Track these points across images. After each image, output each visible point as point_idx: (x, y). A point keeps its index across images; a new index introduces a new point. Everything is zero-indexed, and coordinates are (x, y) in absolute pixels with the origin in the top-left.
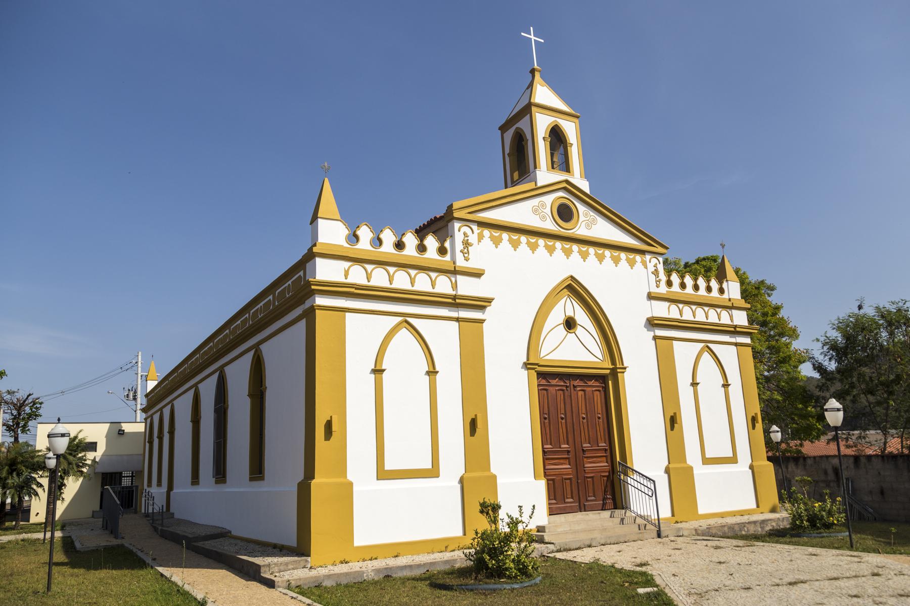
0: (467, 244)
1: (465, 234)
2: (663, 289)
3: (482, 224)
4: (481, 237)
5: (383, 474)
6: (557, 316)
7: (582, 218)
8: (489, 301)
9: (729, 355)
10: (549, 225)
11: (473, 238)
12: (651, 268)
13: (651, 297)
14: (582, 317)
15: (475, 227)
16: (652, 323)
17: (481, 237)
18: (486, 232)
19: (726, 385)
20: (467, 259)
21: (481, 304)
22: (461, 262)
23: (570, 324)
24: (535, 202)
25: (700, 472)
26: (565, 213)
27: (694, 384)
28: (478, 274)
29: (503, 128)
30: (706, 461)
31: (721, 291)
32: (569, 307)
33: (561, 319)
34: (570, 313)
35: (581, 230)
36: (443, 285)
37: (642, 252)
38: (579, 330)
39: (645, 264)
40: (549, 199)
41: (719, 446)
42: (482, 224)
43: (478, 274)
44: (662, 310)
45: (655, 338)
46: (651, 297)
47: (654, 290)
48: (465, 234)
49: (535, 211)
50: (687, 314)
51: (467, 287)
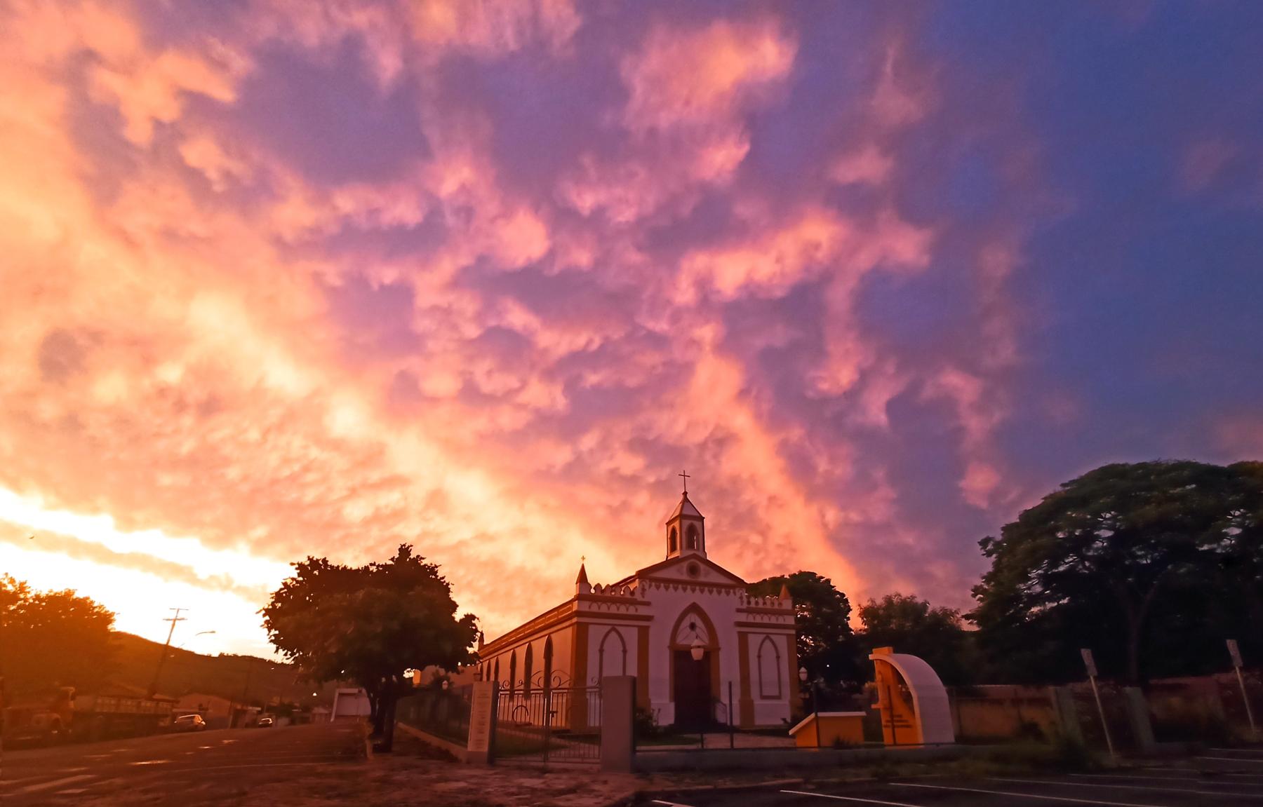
2: (745, 606)
3: (652, 580)
4: (650, 586)
6: (686, 622)
9: (782, 642)
10: (685, 577)
11: (647, 587)
12: (738, 595)
13: (739, 610)
14: (699, 623)
16: (739, 624)
17: (650, 586)
18: (653, 584)
19: (778, 657)
20: (643, 597)
21: (649, 618)
23: (693, 626)
25: (758, 702)
26: (693, 570)
27: (759, 657)
28: (648, 604)
29: (668, 524)
30: (763, 697)
31: (780, 604)
32: (693, 618)
33: (688, 624)
34: (693, 621)
35: (702, 579)
36: (632, 611)
37: (733, 587)
38: (698, 630)
39: (735, 593)
40: (685, 565)
41: (771, 690)
42: (652, 580)
43: (648, 604)
44: (743, 618)
45: (739, 632)
46: (739, 610)
47: (740, 607)
50: (758, 619)
51: (643, 611)
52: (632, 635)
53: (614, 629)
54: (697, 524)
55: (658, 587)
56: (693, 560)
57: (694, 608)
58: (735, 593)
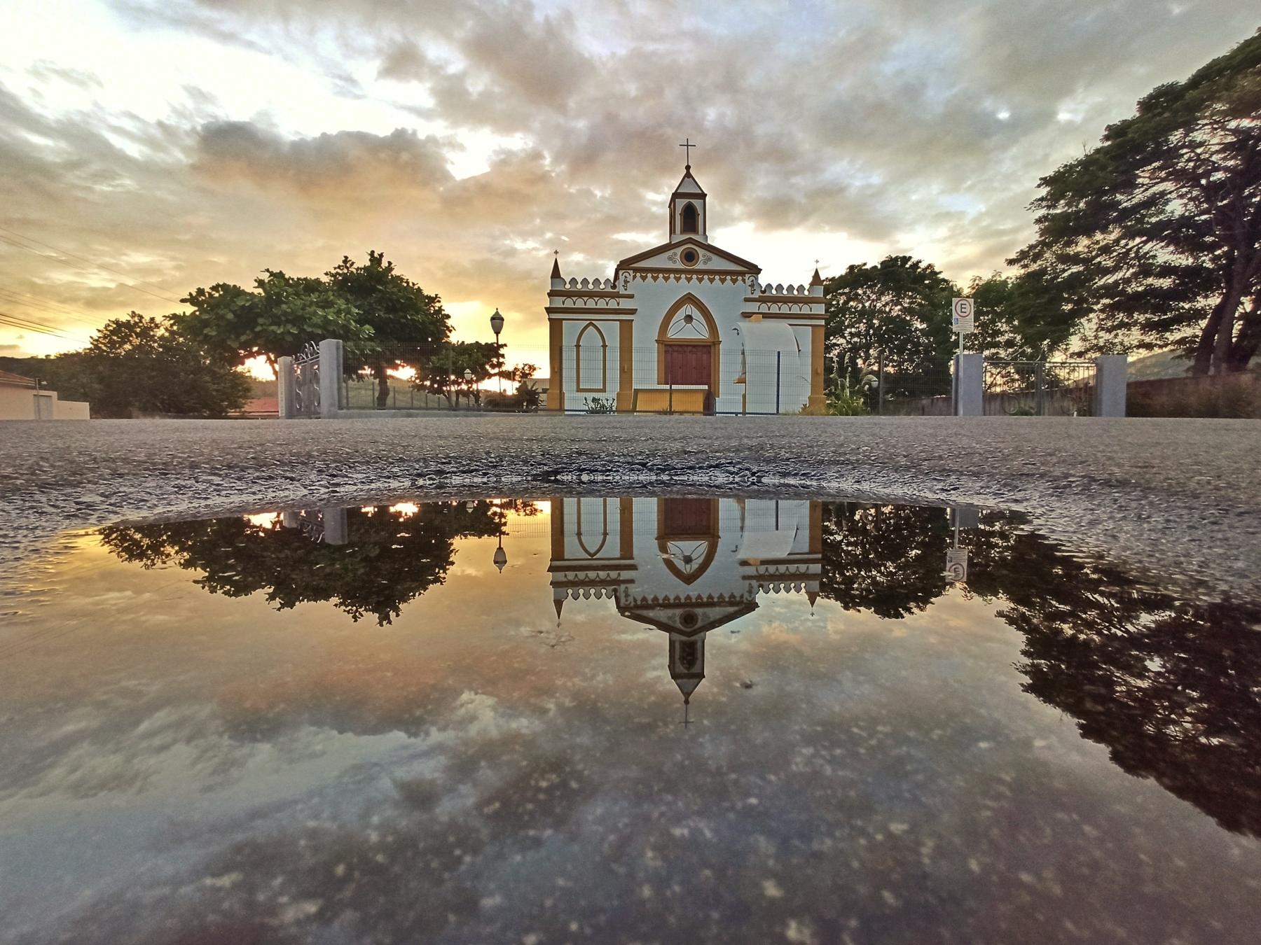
0: (626, 282)
1: (626, 277)
3: (636, 270)
4: (634, 277)
5: (579, 390)
6: (681, 313)
7: (701, 258)
8: (636, 310)
10: (679, 265)
11: (630, 278)
13: (747, 300)
14: (696, 314)
15: (631, 272)
17: (634, 277)
18: (638, 275)
21: (633, 312)
22: (622, 291)
23: (689, 318)
24: (670, 253)
26: (690, 257)
28: (631, 296)
36: (613, 304)
37: (742, 274)
39: (744, 281)
40: (679, 250)
42: (636, 270)
43: (631, 296)
46: (747, 300)
48: (626, 277)
49: (670, 258)
51: (625, 304)
52: (612, 330)
53: (591, 324)
54: (697, 203)
55: (644, 278)
56: (690, 246)
57: (689, 299)
58: (744, 281)
